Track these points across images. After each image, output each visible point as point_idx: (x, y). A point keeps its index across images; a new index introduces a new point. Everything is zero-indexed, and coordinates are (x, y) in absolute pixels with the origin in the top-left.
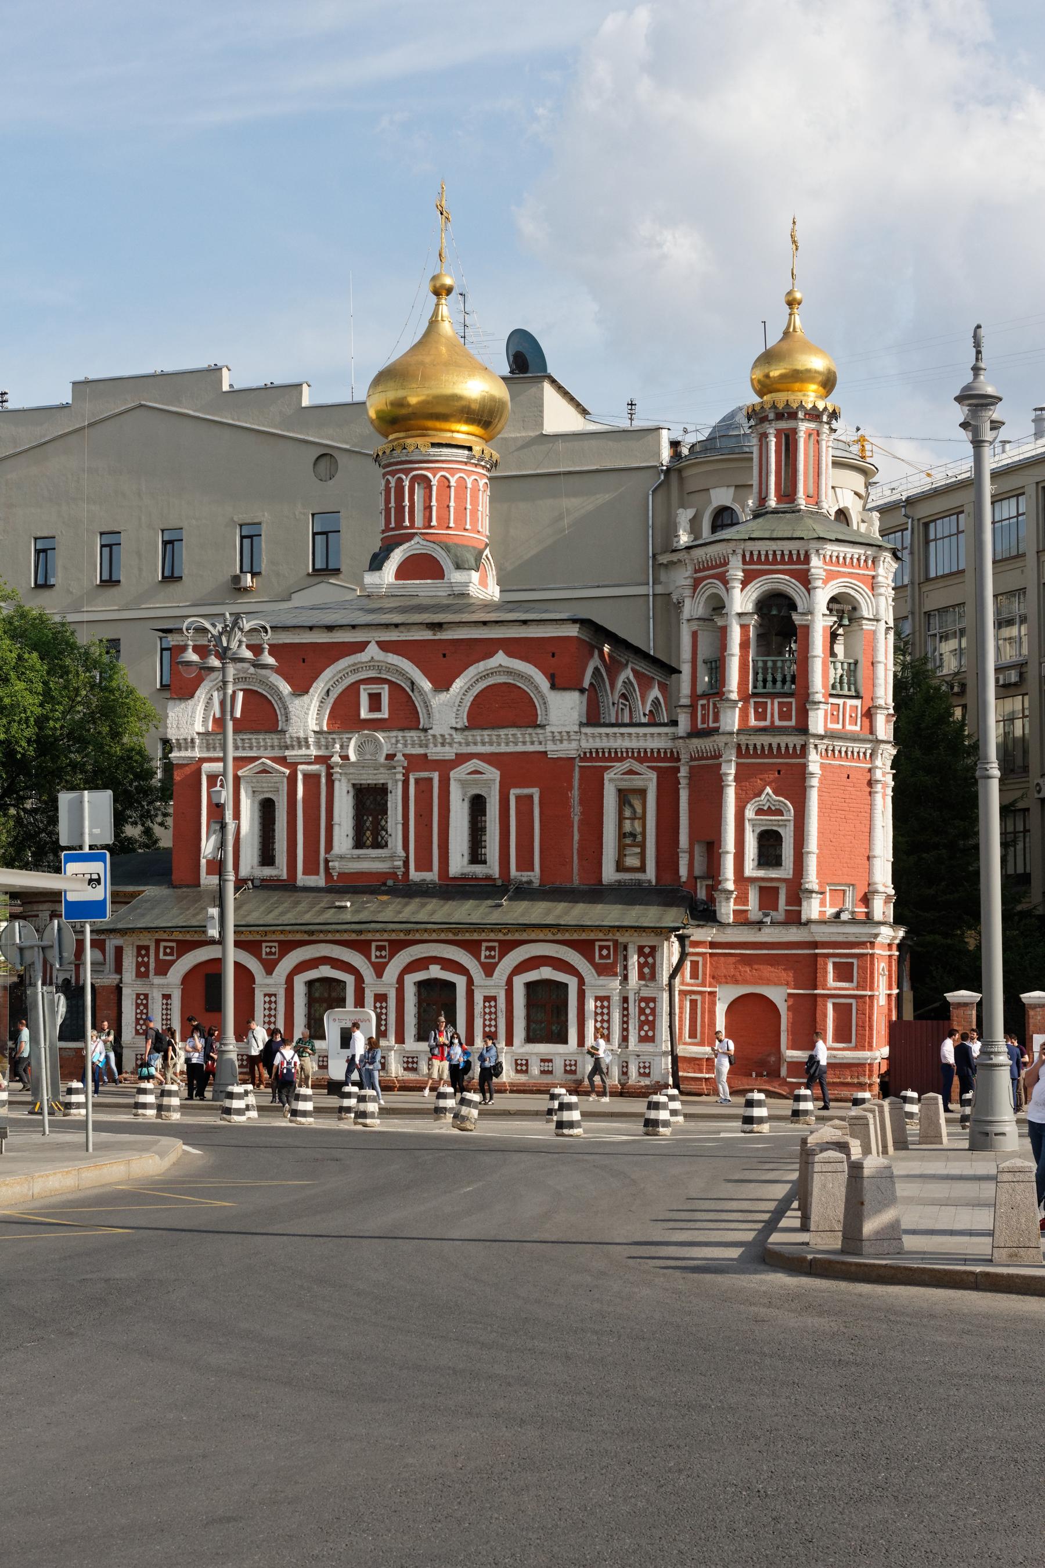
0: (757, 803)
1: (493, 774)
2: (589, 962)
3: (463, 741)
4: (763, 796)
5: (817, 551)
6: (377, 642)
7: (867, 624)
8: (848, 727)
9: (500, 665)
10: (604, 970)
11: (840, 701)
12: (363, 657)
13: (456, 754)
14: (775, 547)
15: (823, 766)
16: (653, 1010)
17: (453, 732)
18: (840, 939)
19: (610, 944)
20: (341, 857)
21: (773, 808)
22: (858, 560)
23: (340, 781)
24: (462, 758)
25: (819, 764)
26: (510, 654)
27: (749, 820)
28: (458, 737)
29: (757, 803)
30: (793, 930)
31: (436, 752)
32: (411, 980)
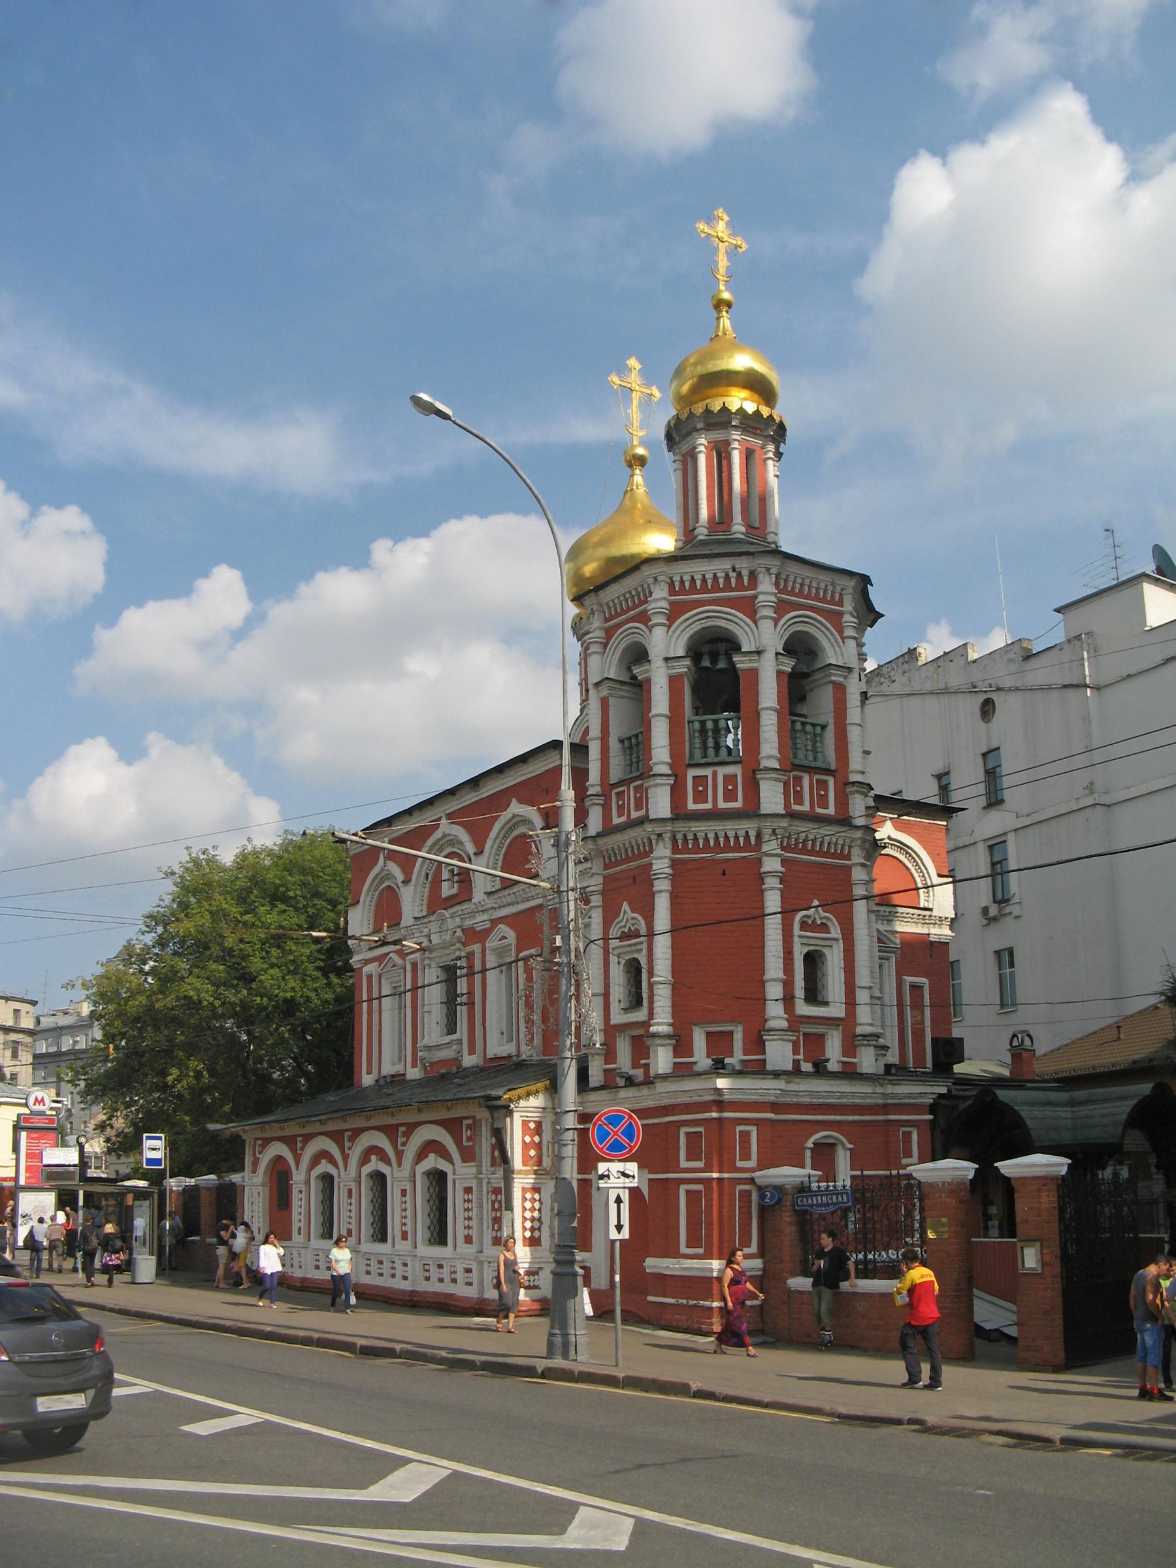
0: (618, 926)
1: (511, 935)
2: (455, 1142)
3: (496, 906)
4: (622, 914)
5: (655, 579)
6: (449, 816)
7: (742, 662)
8: (722, 805)
9: (514, 816)
10: (468, 1155)
11: (708, 772)
12: (438, 834)
13: (491, 920)
14: (623, 591)
15: (674, 864)
16: (500, 1202)
17: (485, 897)
18: (685, 1099)
19: (470, 1121)
20: (428, 1048)
21: (633, 929)
22: (727, 577)
23: (429, 966)
24: (495, 922)
25: (667, 860)
26: (521, 801)
27: (613, 949)
28: (490, 902)
29: (618, 926)
30: (645, 1091)
31: (480, 921)
32: (367, 1169)
